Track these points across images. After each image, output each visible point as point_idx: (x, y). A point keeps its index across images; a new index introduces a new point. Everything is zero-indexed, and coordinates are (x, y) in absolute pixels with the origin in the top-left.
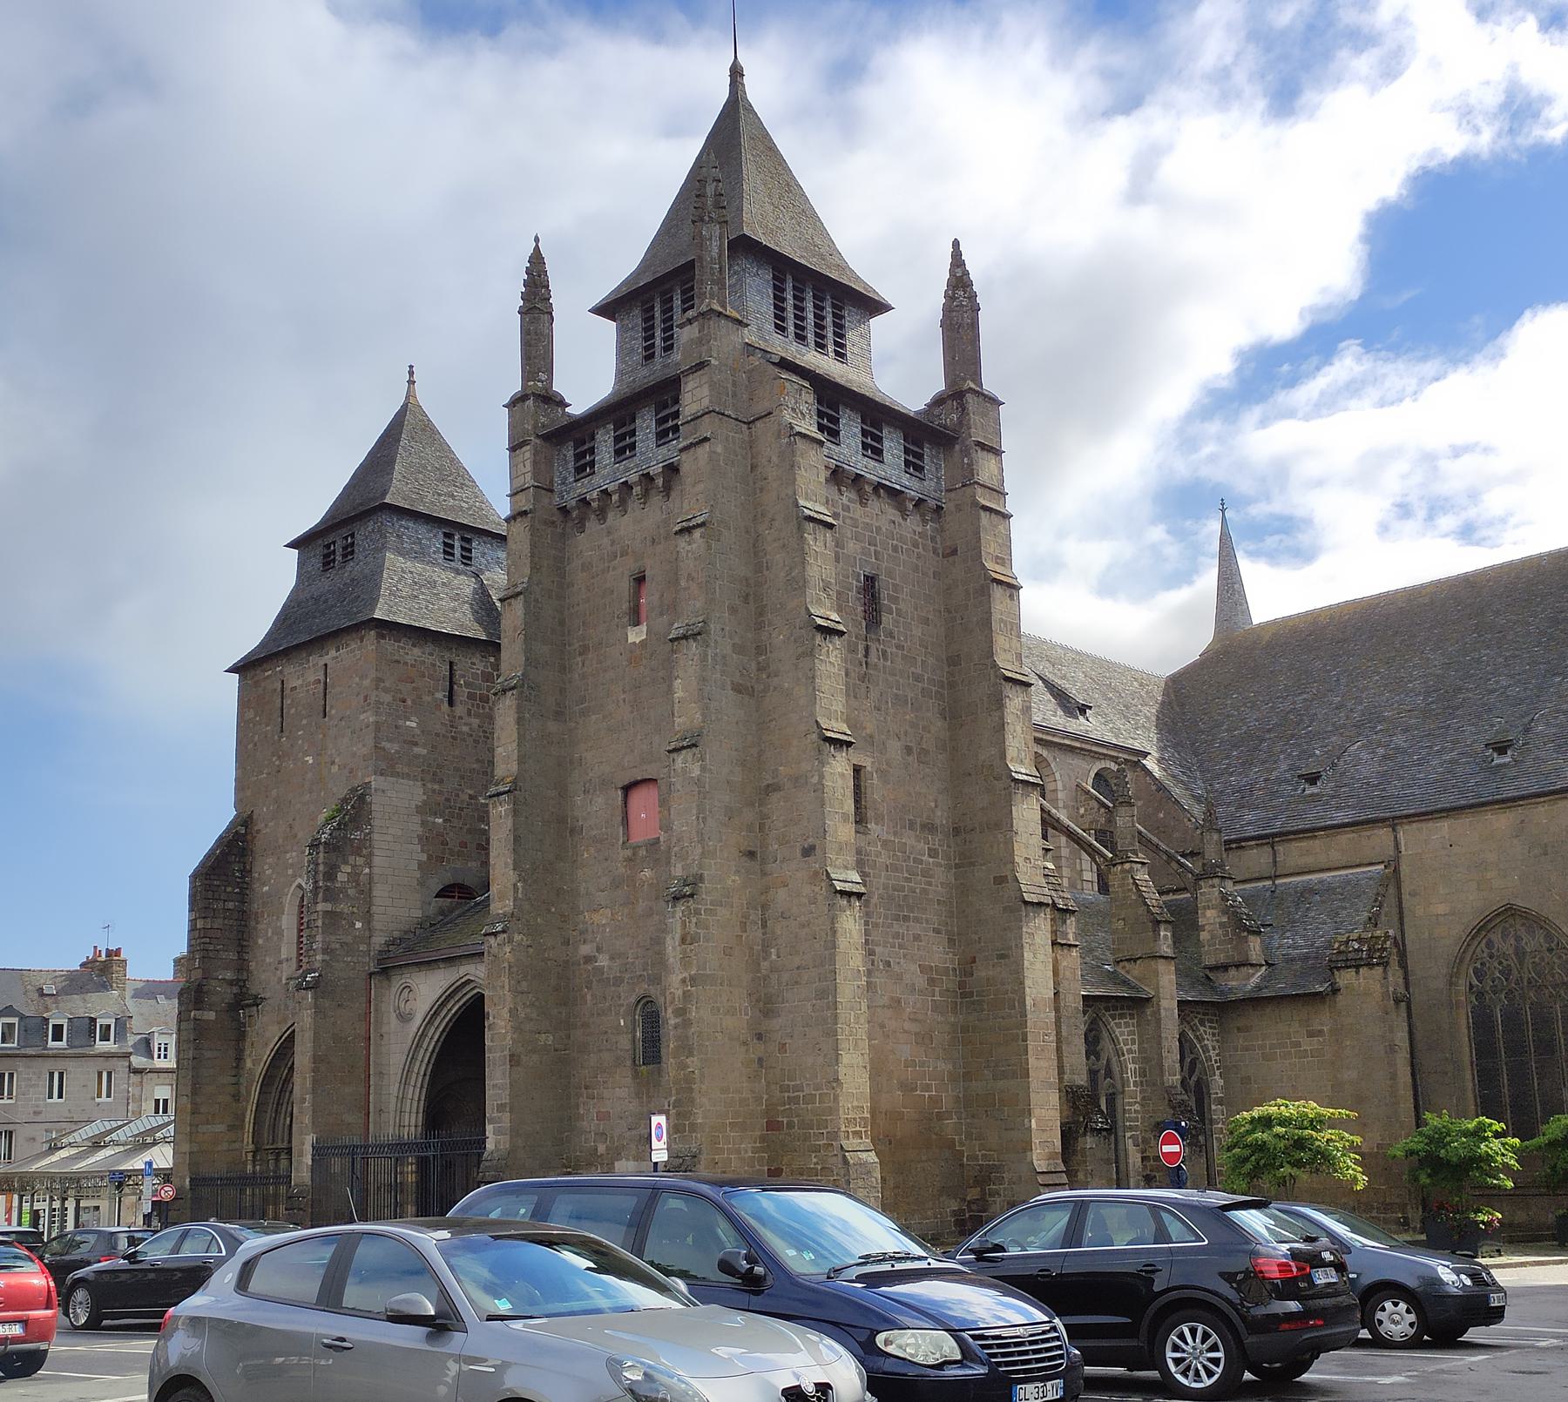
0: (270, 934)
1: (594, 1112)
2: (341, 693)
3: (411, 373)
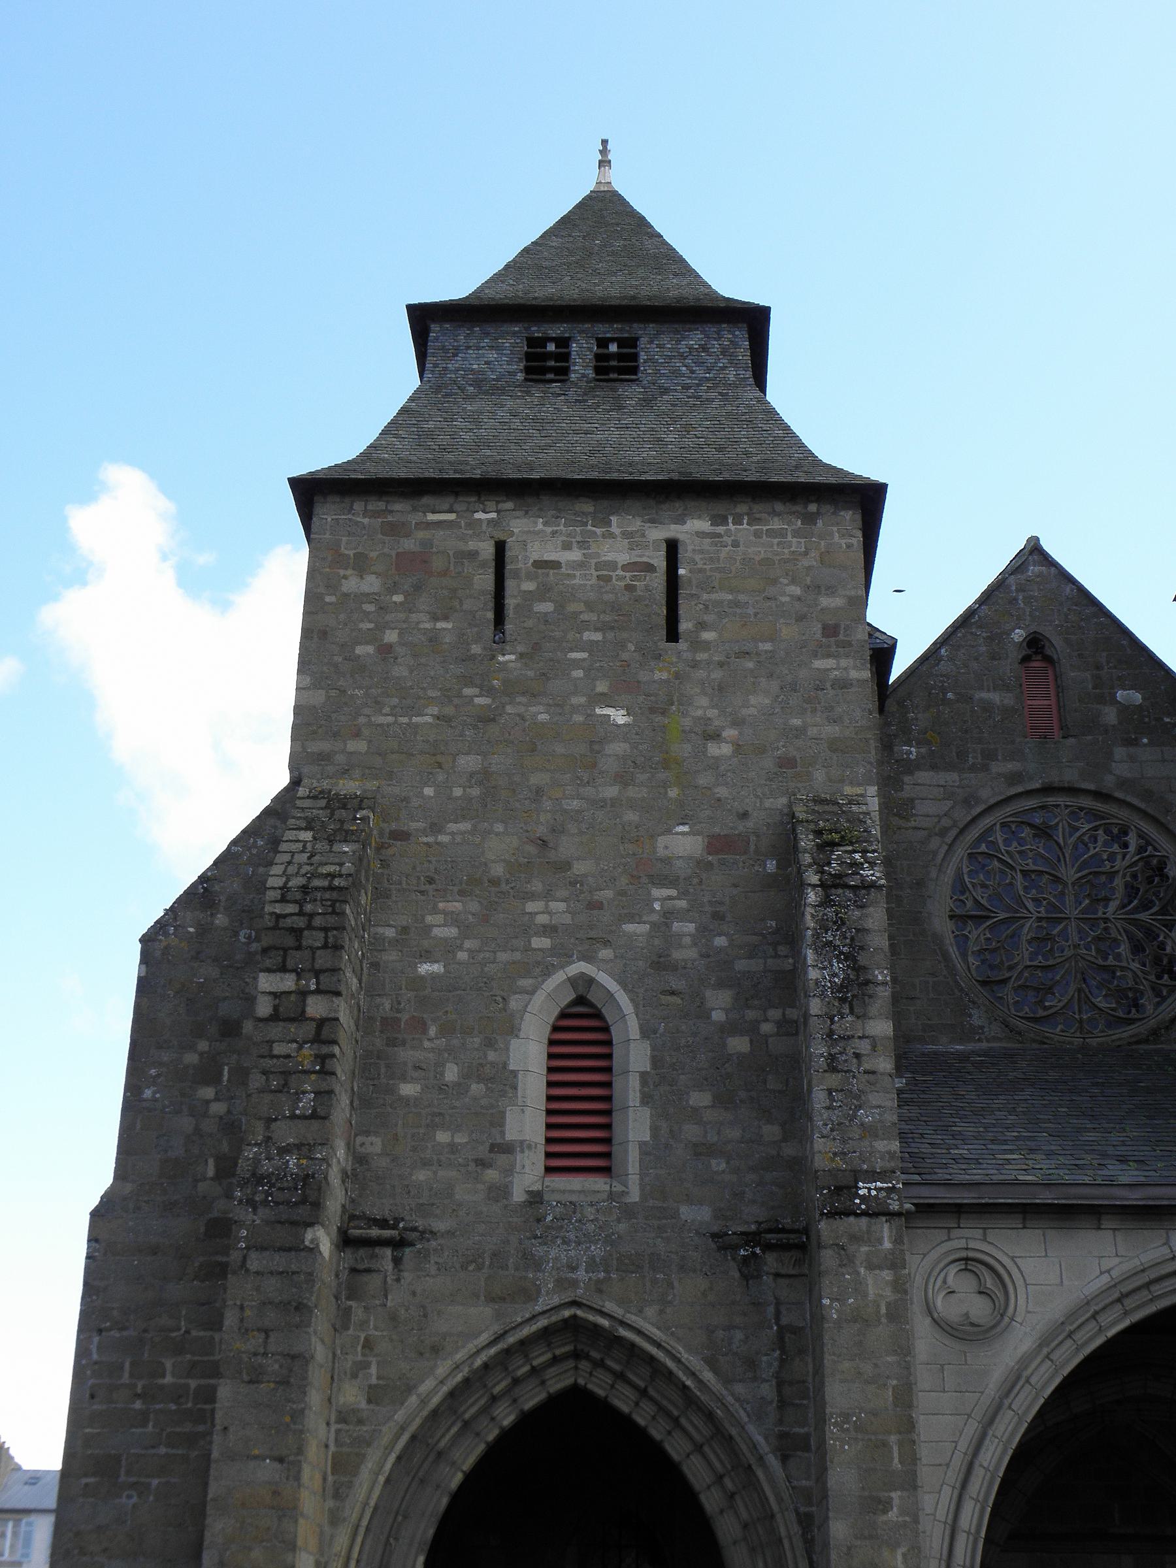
0: (451, 1073)
3: (604, 151)
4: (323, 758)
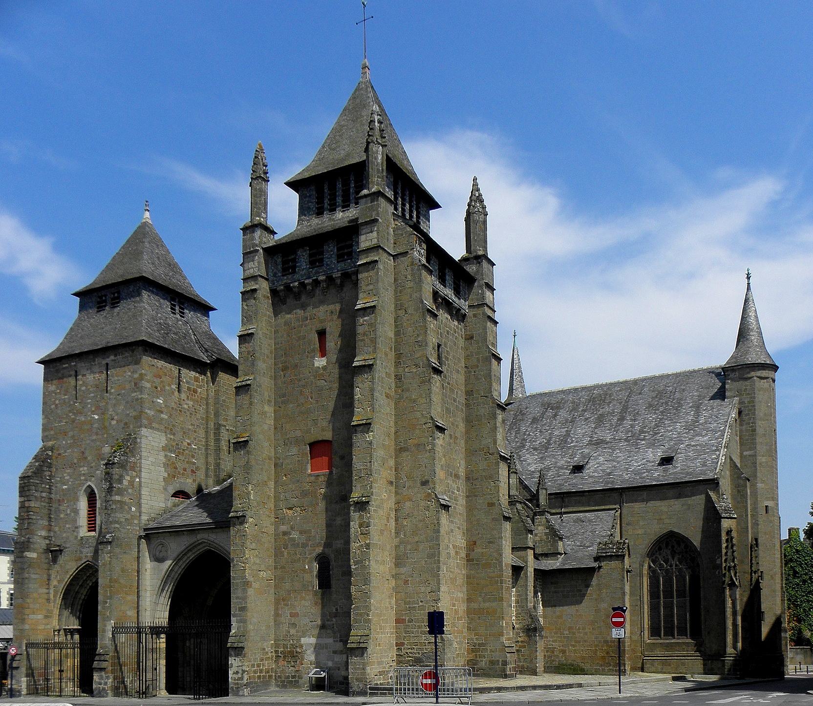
1: (288, 613)
2: (118, 380)
4: (47, 436)
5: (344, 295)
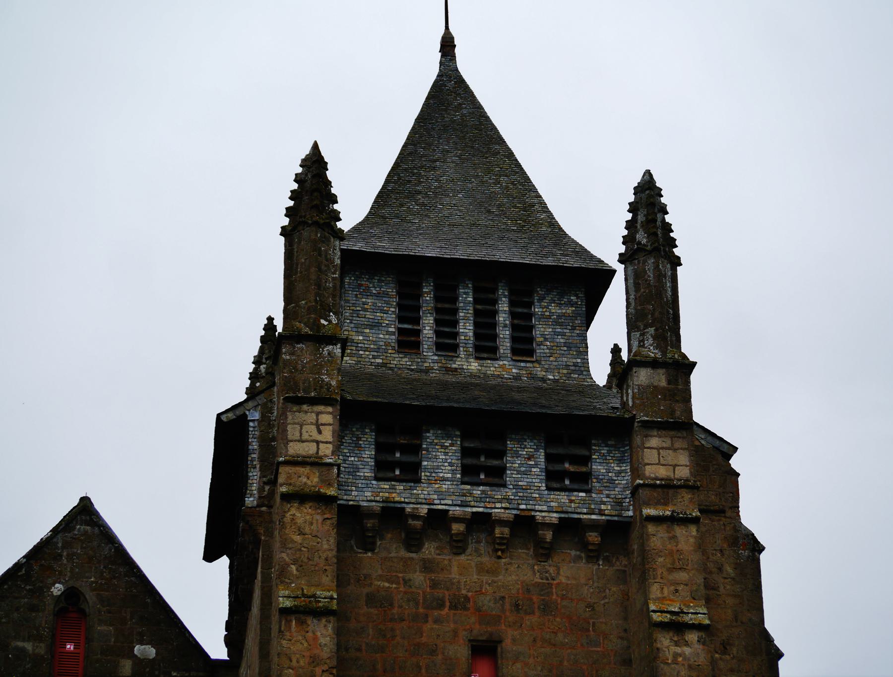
5: (552, 570)
